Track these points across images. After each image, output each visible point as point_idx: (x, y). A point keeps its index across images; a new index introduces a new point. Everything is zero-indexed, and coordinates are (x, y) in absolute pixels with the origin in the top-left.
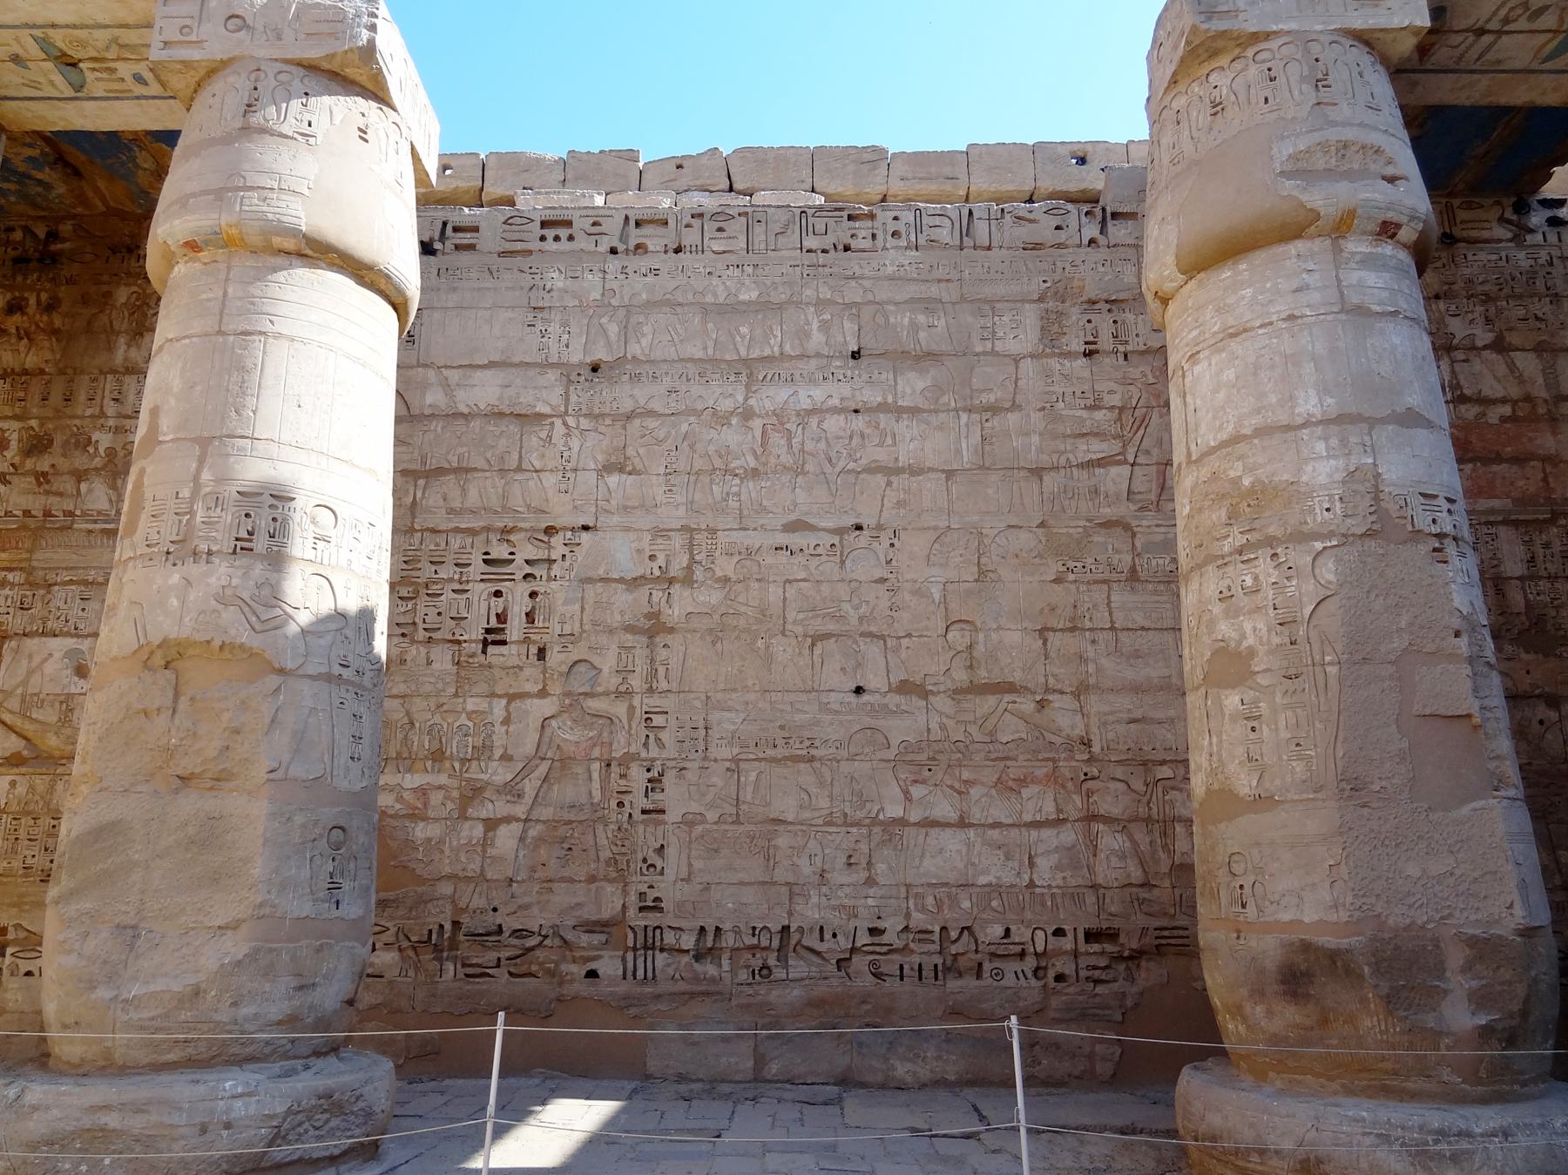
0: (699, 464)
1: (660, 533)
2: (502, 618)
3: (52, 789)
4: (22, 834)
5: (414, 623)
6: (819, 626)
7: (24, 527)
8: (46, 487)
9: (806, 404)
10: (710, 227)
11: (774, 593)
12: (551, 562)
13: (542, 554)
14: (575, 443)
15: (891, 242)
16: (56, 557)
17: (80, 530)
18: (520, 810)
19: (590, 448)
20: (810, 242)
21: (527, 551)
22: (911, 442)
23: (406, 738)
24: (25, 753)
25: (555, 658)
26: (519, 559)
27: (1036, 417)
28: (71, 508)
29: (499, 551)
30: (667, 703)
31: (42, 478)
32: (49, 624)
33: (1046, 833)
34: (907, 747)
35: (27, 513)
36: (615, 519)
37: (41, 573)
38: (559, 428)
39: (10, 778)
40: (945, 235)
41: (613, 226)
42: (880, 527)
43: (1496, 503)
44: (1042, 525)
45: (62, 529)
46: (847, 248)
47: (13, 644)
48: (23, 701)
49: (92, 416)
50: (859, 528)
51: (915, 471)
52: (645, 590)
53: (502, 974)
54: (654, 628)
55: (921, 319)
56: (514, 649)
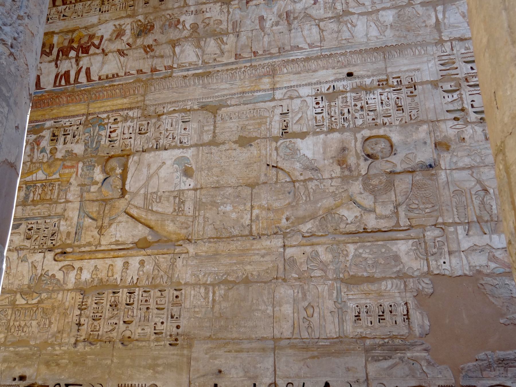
3: (173, 265)
4: (152, 305)
5: (463, 110)
7: (139, 81)
8: (152, 54)
16: (162, 96)
17: (178, 77)
23: (483, 203)
24: (150, 238)
28: (170, 64)
31: (148, 49)
32: (161, 142)
35: (140, 72)
37: (152, 108)
39: (138, 259)
45: (165, 78)
47: (136, 158)
48: (146, 198)
49: (179, 7)
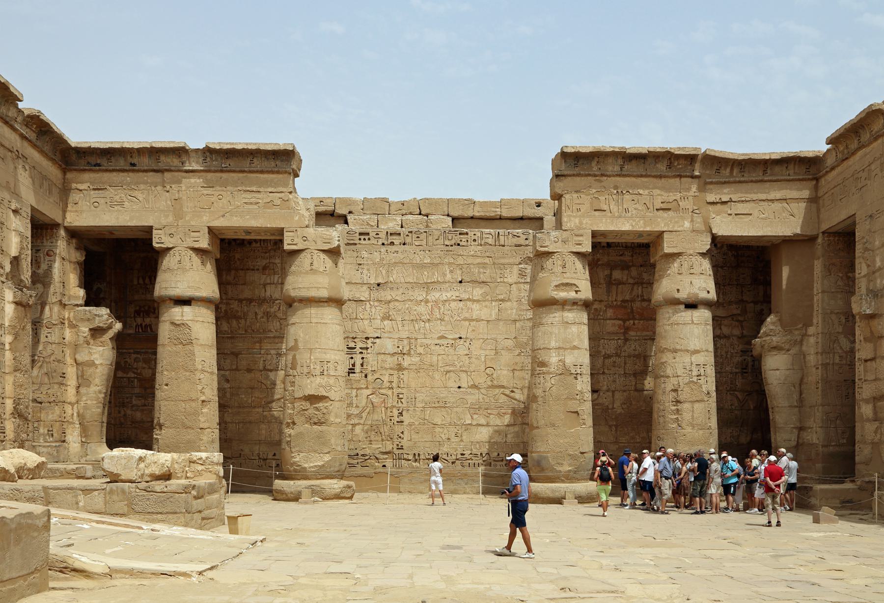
0: (412, 318)
1: (400, 339)
2: (354, 365)
6: (447, 368)
9: (445, 298)
10: (415, 236)
11: (435, 358)
12: (367, 348)
13: (365, 346)
14: (373, 310)
15: (473, 243)
18: (362, 422)
19: (378, 311)
20: (447, 243)
21: (360, 345)
22: (477, 311)
25: (370, 377)
26: (358, 347)
27: (515, 303)
29: (352, 345)
30: (404, 391)
33: (511, 428)
34: (472, 404)
36: (386, 335)
38: (368, 306)
40: (490, 241)
41: (383, 235)
42: (466, 338)
43: (648, 333)
44: (515, 338)
46: (459, 245)
50: (460, 338)
51: (478, 320)
52: (396, 358)
53: (359, 466)
54: (400, 368)
55: (482, 270)
56: (357, 375)
